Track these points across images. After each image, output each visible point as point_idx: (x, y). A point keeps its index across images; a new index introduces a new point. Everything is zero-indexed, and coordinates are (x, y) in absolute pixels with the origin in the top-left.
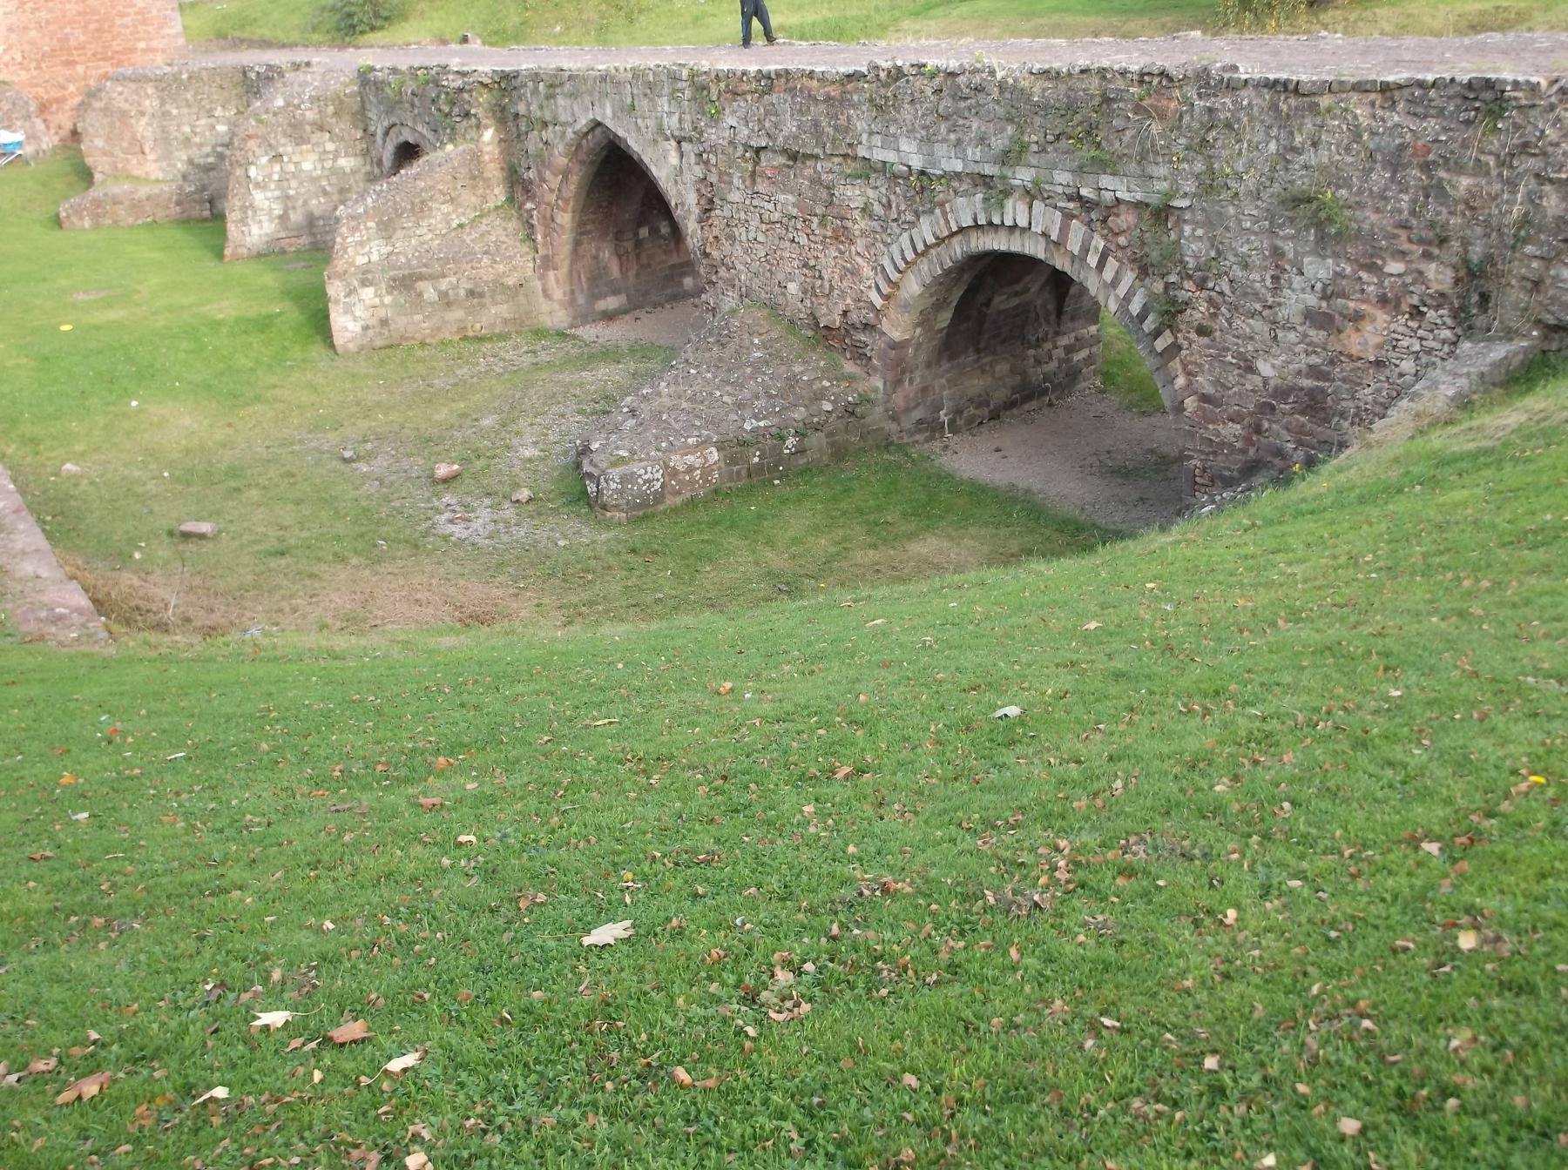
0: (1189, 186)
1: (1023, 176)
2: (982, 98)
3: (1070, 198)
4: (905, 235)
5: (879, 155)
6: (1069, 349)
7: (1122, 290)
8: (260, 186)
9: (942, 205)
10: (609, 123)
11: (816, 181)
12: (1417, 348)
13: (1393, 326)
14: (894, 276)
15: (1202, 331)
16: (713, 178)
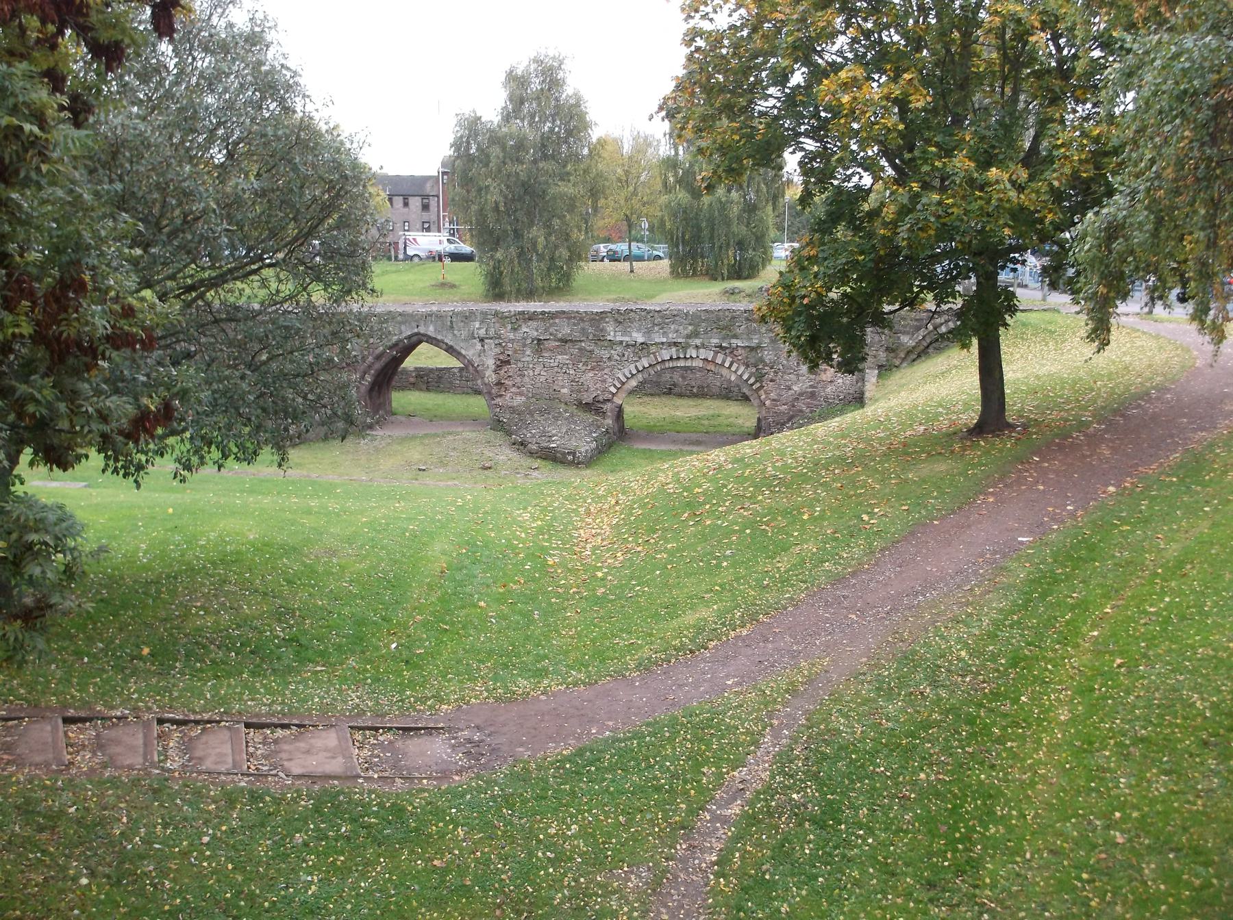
0: (767, 341)
1: (698, 342)
2: (677, 318)
5: (619, 338)
7: (739, 373)
10: (429, 333)
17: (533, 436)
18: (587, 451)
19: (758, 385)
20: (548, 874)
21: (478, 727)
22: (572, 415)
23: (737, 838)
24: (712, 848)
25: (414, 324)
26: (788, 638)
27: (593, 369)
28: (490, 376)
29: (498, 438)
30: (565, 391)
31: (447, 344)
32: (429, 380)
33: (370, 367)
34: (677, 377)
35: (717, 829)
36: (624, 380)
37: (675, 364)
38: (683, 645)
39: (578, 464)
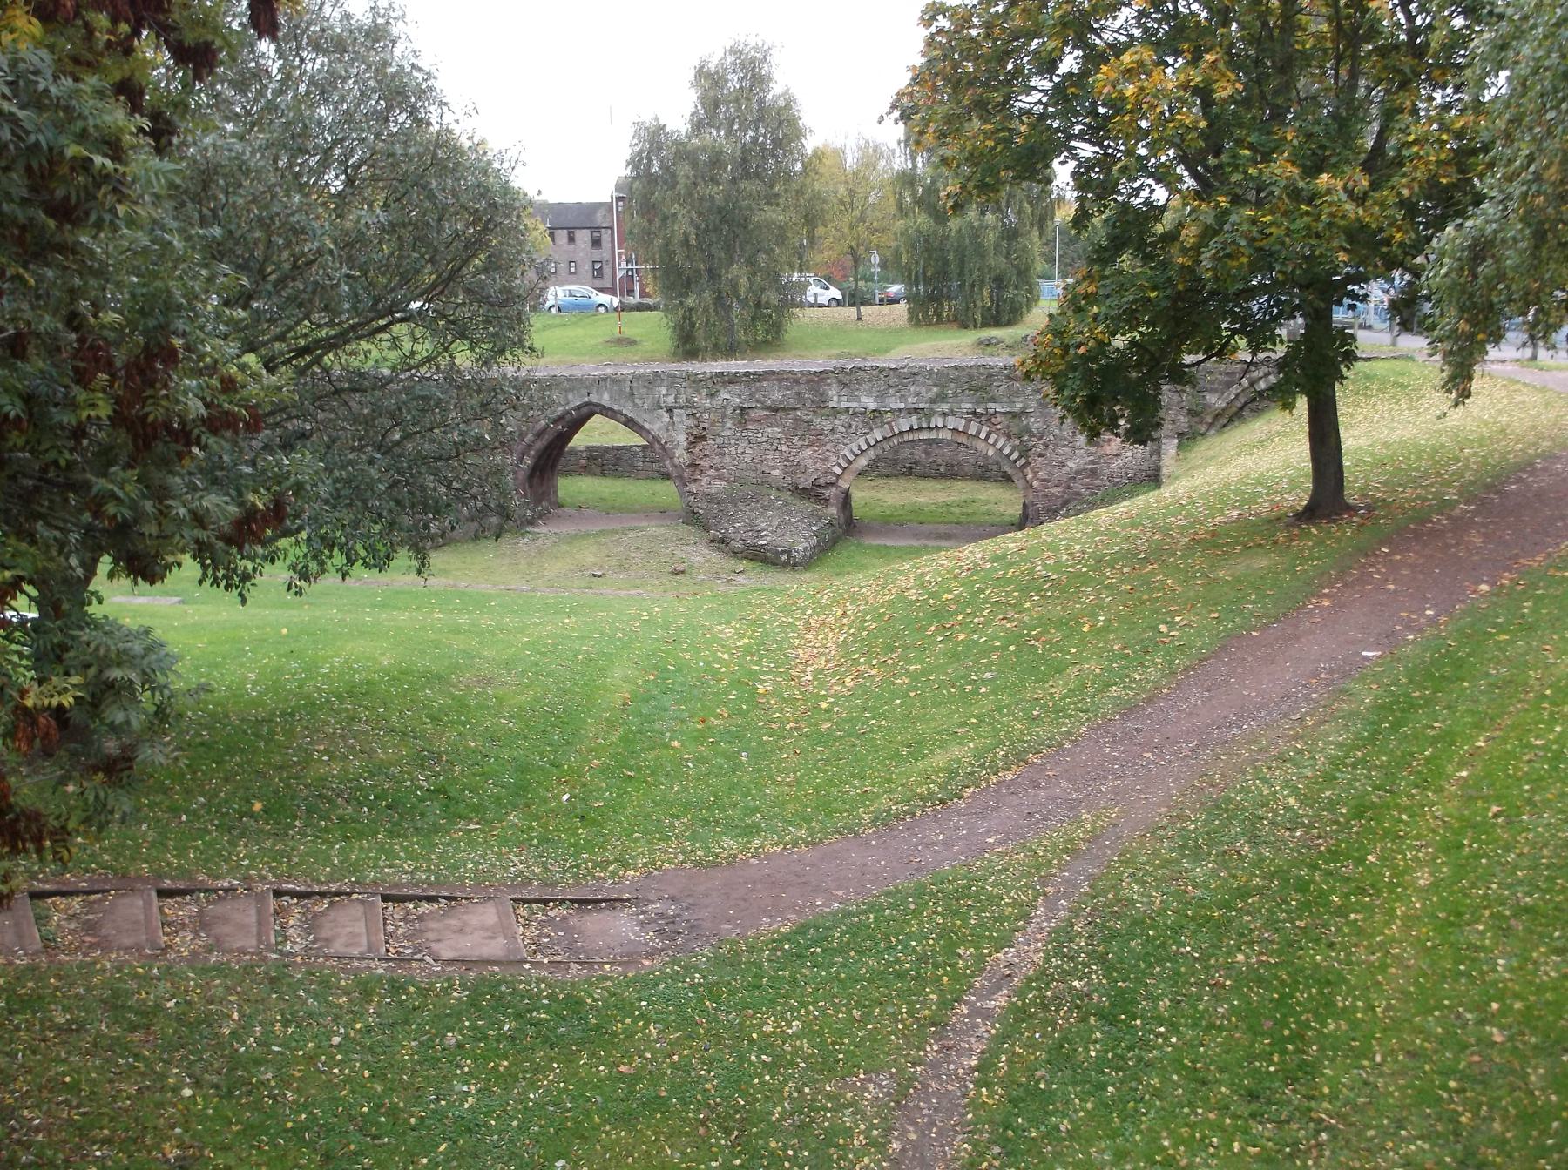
0: (1034, 404)
1: (945, 407)
2: (918, 378)
5: (844, 405)
7: (999, 446)
9: (888, 423)
10: (603, 403)
11: (796, 420)
15: (1041, 455)
17: (737, 531)
18: (805, 549)
19: (1023, 461)
20: (763, 1083)
21: (673, 899)
22: (786, 504)
23: (1003, 1037)
24: (971, 1049)
25: (584, 392)
26: (1064, 784)
27: (811, 444)
28: (681, 455)
29: (692, 533)
30: (776, 473)
31: (626, 416)
32: (605, 462)
33: (529, 446)
34: (919, 453)
35: (978, 1026)
36: (851, 457)
37: (916, 436)
38: (931, 793)
39: (795, 565)
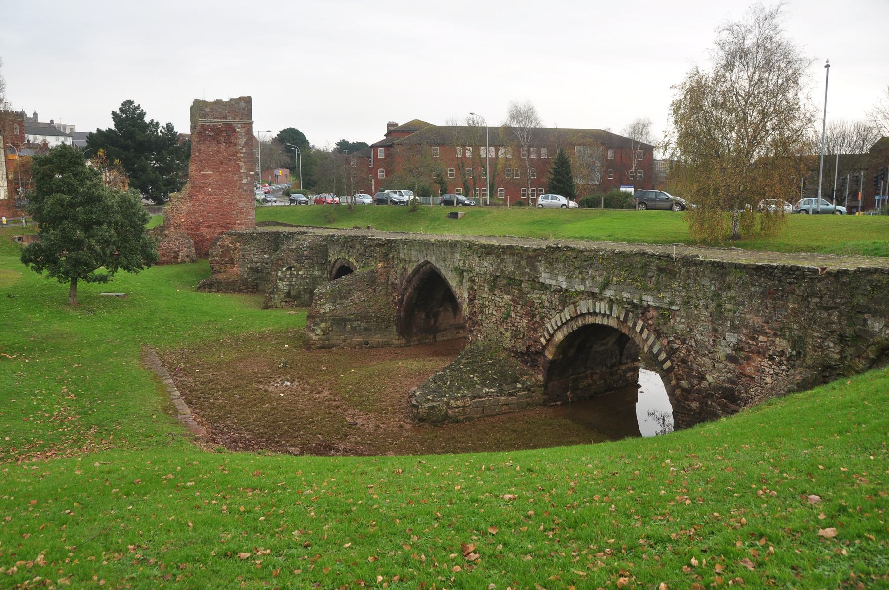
0: (678, 301)
3: (629, 304)
4: (558, 315)
5: (548, 282)
6: (625, 372)
7: (650, 342)
8: (281, 279)
10: (433, 262)
12: (772, 372)
13: (762, 363)
14: (551, 332)
16: (475, 287)
